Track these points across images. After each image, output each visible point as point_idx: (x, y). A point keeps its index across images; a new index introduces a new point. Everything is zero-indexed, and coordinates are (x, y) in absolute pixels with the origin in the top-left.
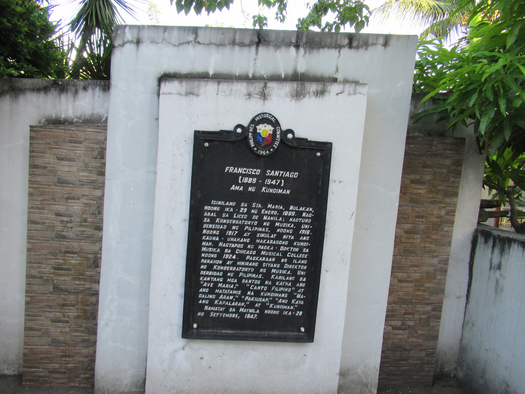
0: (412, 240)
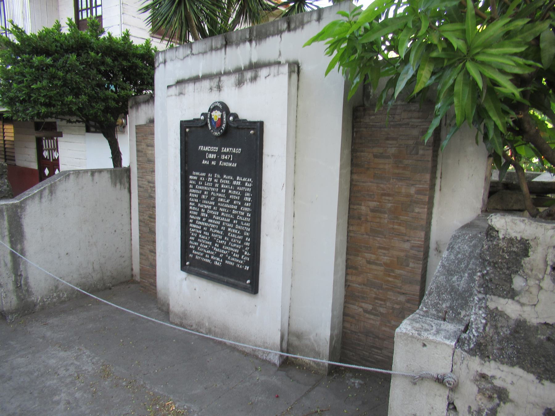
0: (378, 220)
